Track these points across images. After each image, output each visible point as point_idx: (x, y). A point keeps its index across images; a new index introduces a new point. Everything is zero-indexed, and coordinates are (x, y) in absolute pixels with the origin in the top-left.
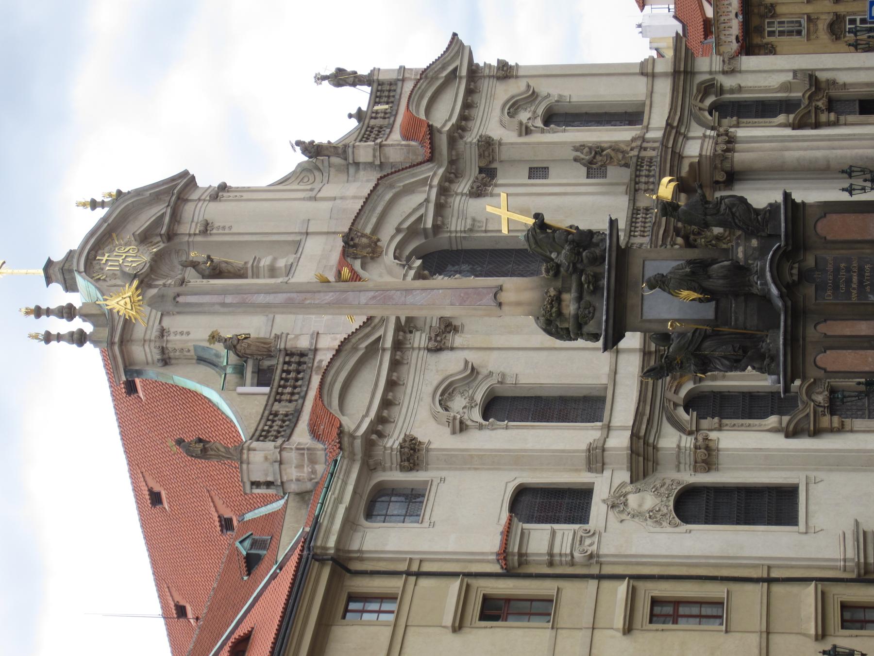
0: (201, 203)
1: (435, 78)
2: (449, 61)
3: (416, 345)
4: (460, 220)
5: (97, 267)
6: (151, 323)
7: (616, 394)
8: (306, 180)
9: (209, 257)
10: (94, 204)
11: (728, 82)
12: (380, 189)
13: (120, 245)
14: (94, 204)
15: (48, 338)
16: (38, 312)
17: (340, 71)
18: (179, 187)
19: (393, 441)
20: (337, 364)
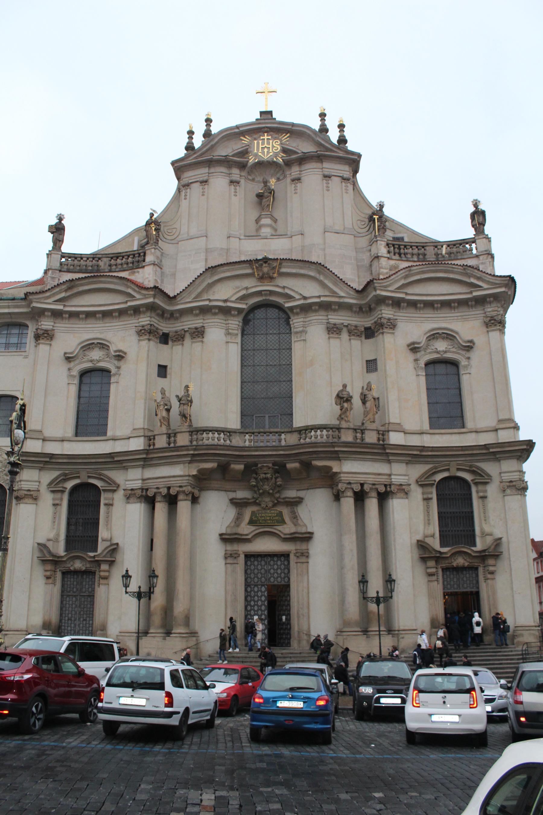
0: (321, 170)
1: (470, 276)
2: (485, 280)
3: (140, 320)
4: (302, 323)
5: (255, 136)
6: (193, 178)
7: (99, 442)
8: (363, 223)
9: (273, 190)
10: (323, 115)
11: (492, 490)
12: (314, 267)
13: (281, 141)
14: (323, 115)
15: (191, 133)
16: (208, 121)
17: (483, 213)
18: (333, 154)
19: (46, 324)
20: (115, 280)
